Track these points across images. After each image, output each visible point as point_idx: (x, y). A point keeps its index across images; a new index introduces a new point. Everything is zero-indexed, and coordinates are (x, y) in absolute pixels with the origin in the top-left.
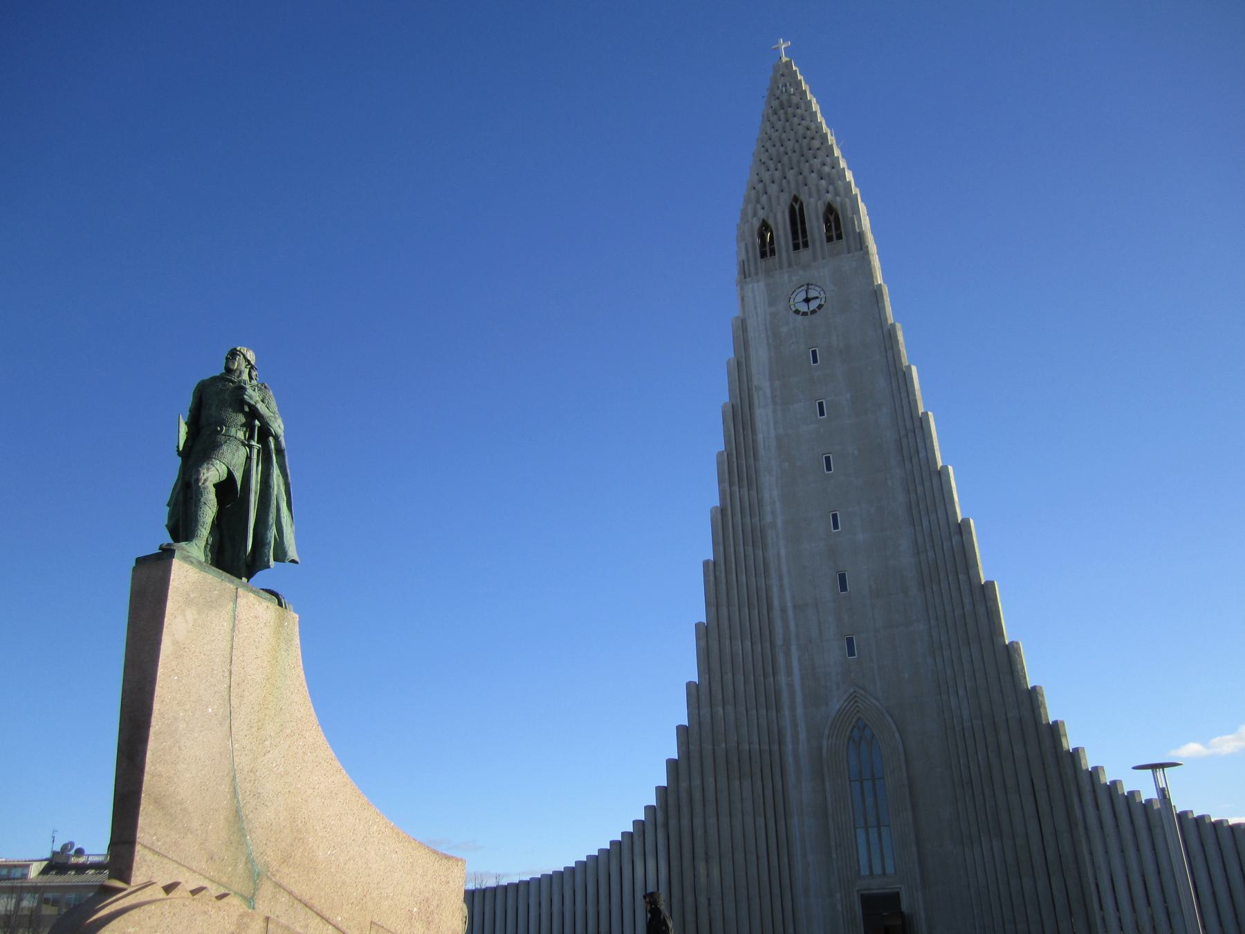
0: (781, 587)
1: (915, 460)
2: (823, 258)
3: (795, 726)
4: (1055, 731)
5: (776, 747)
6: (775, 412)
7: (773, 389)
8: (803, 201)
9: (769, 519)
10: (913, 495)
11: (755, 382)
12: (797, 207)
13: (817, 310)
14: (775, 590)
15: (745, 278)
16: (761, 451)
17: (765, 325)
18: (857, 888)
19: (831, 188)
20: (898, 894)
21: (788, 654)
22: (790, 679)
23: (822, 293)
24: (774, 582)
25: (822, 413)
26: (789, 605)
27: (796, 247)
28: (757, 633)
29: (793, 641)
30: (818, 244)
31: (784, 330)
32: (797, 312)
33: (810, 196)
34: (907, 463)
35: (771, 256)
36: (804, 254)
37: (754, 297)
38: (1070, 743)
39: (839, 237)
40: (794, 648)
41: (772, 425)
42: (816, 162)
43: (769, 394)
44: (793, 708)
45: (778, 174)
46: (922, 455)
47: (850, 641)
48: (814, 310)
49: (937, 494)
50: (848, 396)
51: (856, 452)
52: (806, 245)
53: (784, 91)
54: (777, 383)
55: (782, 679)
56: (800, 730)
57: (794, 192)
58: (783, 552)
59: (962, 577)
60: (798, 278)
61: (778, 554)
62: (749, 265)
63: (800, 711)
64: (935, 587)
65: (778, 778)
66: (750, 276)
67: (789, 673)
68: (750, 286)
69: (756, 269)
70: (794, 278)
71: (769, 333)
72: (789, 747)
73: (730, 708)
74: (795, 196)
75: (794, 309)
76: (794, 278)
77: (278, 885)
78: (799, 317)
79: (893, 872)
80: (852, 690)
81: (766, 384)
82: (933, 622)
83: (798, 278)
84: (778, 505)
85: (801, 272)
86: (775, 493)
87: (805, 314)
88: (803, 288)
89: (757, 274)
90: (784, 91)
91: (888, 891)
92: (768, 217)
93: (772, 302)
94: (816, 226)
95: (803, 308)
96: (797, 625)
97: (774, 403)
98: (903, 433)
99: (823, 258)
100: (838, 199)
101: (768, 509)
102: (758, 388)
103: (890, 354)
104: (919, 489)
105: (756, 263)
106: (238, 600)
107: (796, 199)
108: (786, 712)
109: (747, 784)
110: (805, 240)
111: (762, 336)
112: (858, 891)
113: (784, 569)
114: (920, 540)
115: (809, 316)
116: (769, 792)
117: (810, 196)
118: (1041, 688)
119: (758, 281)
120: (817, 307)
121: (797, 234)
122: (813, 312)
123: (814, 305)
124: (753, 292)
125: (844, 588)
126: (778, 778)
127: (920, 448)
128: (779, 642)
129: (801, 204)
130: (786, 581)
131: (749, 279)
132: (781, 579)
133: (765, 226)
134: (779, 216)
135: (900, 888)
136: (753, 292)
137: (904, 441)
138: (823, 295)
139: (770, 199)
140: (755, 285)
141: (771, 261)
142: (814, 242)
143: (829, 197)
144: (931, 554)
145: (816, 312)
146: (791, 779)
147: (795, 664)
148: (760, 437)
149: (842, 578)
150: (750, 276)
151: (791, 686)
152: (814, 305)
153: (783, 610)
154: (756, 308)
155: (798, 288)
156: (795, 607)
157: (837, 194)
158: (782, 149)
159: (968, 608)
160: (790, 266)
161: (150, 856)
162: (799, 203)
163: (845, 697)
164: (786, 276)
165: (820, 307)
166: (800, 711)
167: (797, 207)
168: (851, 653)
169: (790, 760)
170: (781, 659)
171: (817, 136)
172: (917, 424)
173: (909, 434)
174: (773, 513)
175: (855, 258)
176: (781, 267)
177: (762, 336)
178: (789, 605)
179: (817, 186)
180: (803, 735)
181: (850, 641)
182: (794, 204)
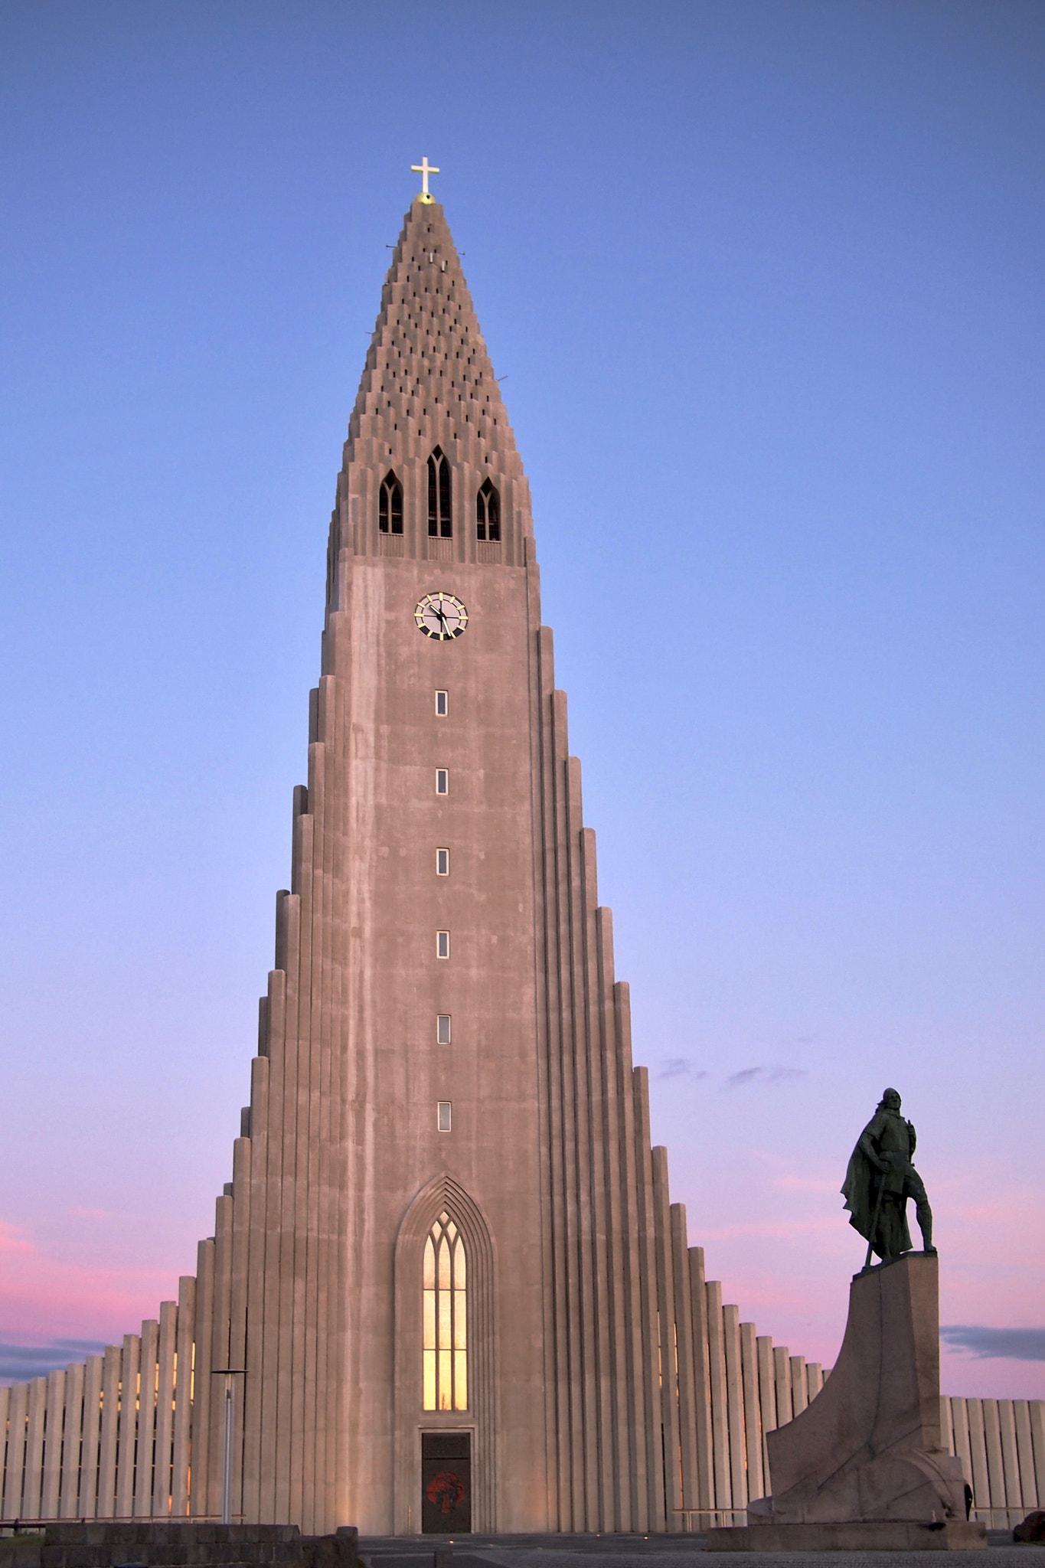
0: (361, 1021)
2: (473, 561)
3: (360, 1211)
5: (335, 1237)
6: (377, 769)
7: (378, 735)
8: (450, 460)
9: (354, 922)
10: (551, 933)
11: (354, 720)
12: (437, 464)
14: (352, 1024)
15: (356, 554)
16: (353, 824)
17: (378, 636)
18: (419, 1426)
19: (494, 455)
24: (352, 1013)
25: (442, 789)
26: (369, 1047)
27: (432, 531)
28: (326, 1081)
29: (370, 1097)
30: (467, 533)
31: (404, 652)
32: (425, 630)
33: (465, 459)
34: (550, 889)
35: (394, 531)
37: (366, 587)
38: (709, 1274)
39: (495, 534)
40: (369, 1107)
41: (371, 786)
42: (477, 404)
43: (371, 740)
44: (360, 1187)
45: (418, 402)
46: (576, 883)
50: (481, 773)
51: (482, 857)
52: (447, 532)
53: (431, 261)
54: (385, 729)
55: (350, 1145)
58: (368, 973)
59: (610, 1056)
60: (432, 578)
61: (362, 973)
62: (364, 536)
63: (369, 1192)
64: (567, 1059)
65: (334, 1277)
66: (364, 553)
67: (360, 1141)
68: (362, 568)
69: (375, 544)
70: (427, 578)
71: (382, 649)
72: (350, 1239)
73: (289, 1179)
74: (438, 447)
76: (427, 578)
79: (465, 1409)
80: (443, 1175)
81: (369, 726)
82: (555, 1103)
83: (432, 578)
84: (368, 904)
85: (437, 572)
86: (366, 887)
87: (435, 636)
88: (435, 597)
90: (431, 261)
92: (400, 468)
93: (390, 606)
94: (464, 508)
95: (434, 626)
96: (376, 1077)
97: (378, 757)
98: (549, 845)
100: (503, 477)
101: (353, 908)
102: (359, 729)
104: (563, 928)
105: (375, 535)
107: (437, 451)
108: (351, 1192)
109: (300, 1285)
110: (445, 519)
111: (371, 651)
114: (553, 992)
118: (684, 1206)
119: (374, 565)
121: (435, 510)
124: (365, 580)
128: (351, 1096)
129: (445, 466)
130: (368, 1014)
131: (359, 557)
132: (361, 1010)
133: (391, 478)
134: (417, 471)
135: (473, 1428)
136: (365, 580)
139: (405, 442)
140: (369, 570)
141: (390, 537)
142: (461, 529)
143: (491, 470)
146: (349, 1281)
148: (353, 801)
150: (364, 553)
151: (360, 1158)
152: (450, 627)
153: (361, 1053)
154: (366, 605)
155: (430, 595)
156: (376, 1052)
158: (426, 362)
159: (611, 1094)
160: (424, 557)
163: (434, 1181)
164: (415, 572)
165: (458, 632)
166: (369, 1192)
167: (437, 464)
169: (350, 1254)
170: (351, 1119)
172: (574, 841)
174: (360, 916)
175: (514, 576)
177: (371, 651)
178: (369, 1047)
180: (369, 1225)
182: (434, 457)
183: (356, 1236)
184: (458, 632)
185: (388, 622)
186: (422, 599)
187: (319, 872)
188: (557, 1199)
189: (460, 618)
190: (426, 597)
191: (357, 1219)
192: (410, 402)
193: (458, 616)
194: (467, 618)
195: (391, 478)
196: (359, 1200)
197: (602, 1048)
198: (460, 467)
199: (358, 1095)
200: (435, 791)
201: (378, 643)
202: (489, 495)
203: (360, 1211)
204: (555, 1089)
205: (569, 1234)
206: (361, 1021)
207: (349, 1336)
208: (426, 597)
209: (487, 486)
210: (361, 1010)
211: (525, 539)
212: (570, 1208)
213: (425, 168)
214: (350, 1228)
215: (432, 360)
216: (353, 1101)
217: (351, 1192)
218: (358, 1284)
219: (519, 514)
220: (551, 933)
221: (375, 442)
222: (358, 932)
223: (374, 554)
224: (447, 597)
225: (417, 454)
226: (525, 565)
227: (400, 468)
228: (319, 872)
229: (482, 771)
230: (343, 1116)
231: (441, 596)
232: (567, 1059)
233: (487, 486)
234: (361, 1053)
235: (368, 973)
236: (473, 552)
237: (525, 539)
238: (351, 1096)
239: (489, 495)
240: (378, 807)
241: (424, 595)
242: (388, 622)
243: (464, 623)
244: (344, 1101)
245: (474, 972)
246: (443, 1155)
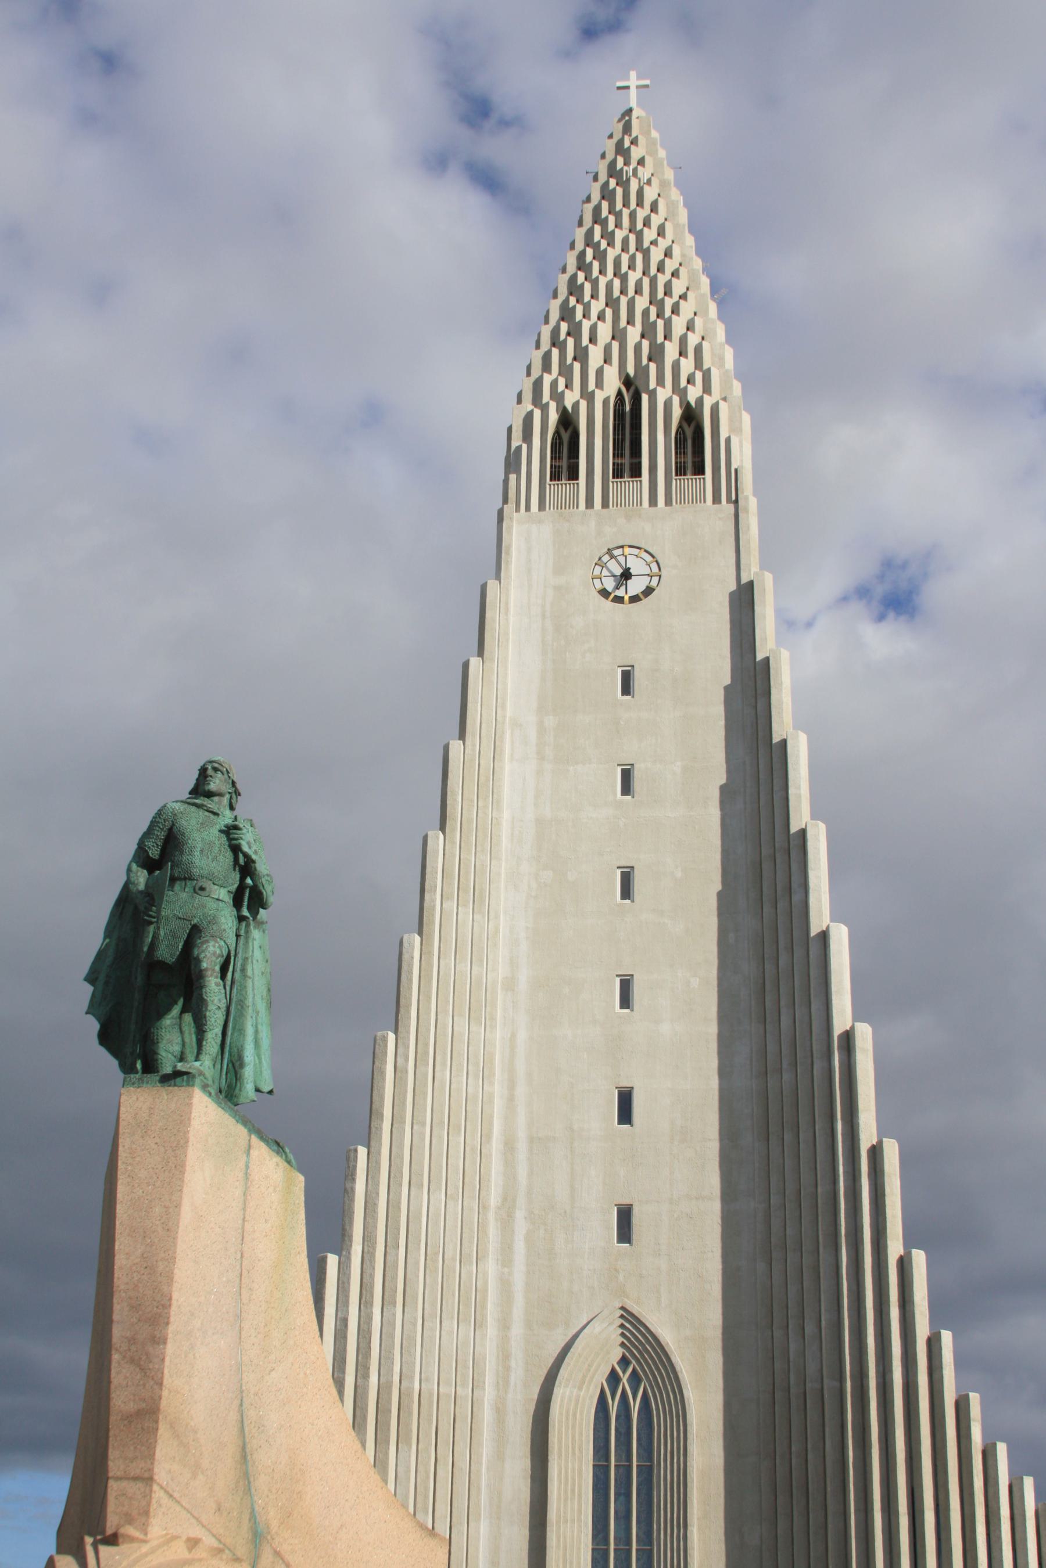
1: (782, 905)
5: (465, 1392)
7: (541, 730)
10: (769, 967)
11: (509, 713)
13: (641, 596)
22: (506, 1270)
23: (654, 566)
24: (498, 1089)
26: (522, 1134)
29: (521, 1201)
40: (520, 1215)
44: (505, 1324)
46: (796, 898)
48: (637, 595)
51: (679, 874)
54: (550, 721)
55: (491, 1267)
56: (513, 1364)
61: (513, 1036)
63: (517, 1330)
64: (788, 1137)
65: (463, 1448)
66: (528, 508)
72: (488, 1394)
75: (599, 586)
77: (277, 1554)
78: (608, 604)
82: (775, 1200)
93: (559, 569)
97: (541, 757)
99: (668, 502)
100: (708, 402)
106: (252, 1151)
108: (491, 1330)
110: (635, 461)
113: (521, 1067)
114: (771, 1048)
115: (627, 607)
116: (444, 1473)
117: (661, 382)
122: (634, 599)
123: (636, 586)
126: (463, 1448)
127: (794, 885)
128: (494, 1199)
133: (567, 421)
137: (767, 867)
141: (565, 486)
143: (693, 394)
144: (786, 1076)
146: (486, 1450)
148: (506, 815)
152: (636, 586)
156: (531, 1140)
157: (707, 389)
160: (605, 504)
161: (165, 1500)
164: (593, 524)
165: (648, 591)
169: (487, 1415)
171: (683, 271)
173: (777, 855)
176: (590, 503)
178: (522, 1134)
179: (676, 367)
180: (517, 1375)
183: (498, 1391)
185: (557, 588)
187: (451, 905)
188: (778, 1334)
191: (500, 1368)
192: (593, 329)
193: (648, 572)
195: (567, 421)
196: (504, 1342)
198: (653, 395)
199: (505, 1199)
200: (615, 795)
201: (544, 616)
202: (693, 425)
203: (505, 1356)
204: (774, 1179)
205: (792, 1382)
206: (511, 1099)
207: (483, 1528)
209: (691, 416)
210: (512, 1085)
211: (736, 470)
212: (793, 1347)
213: (633, 81)
214: (489, 1379)
215: (624, 279)
216: (499, 1208)
217: (491, 1330)
218: (499, 1456)
219: (728, 441)
220: (769, 967)
221: (547, 379)
222: (510, 985)
223: (542, 506)
225: (599, 384)
226: (736, 501)
227: (576, 405)
228: (451, 905)
229: (679, 763)
230: (482, 1226)
232: (788, 1137)
233: (691, 416)
234: (509, 1146)
235: (522, 1035)
237: (736, 470)
238: (494, 1199)
239: (693, 425)
240: (539, 822)
242: (557, 588)
244: (482, 1207)
245: (665, 1028)
246: (621, 1277)
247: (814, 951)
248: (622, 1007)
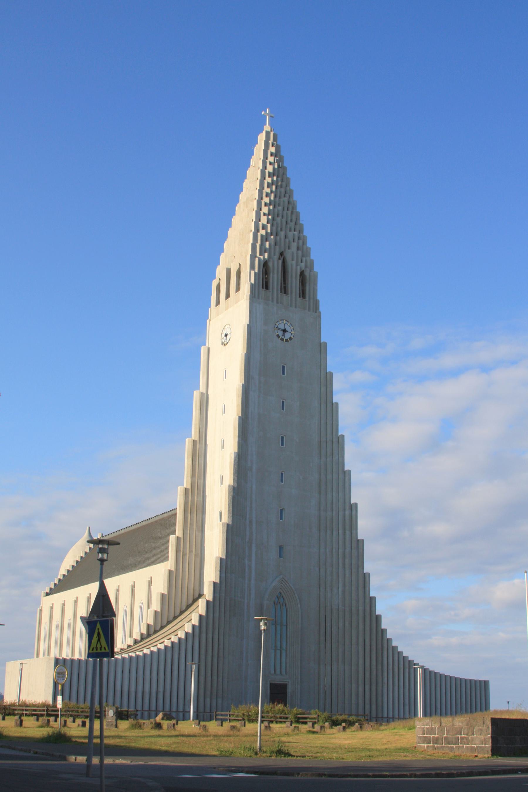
4: (378, 618)
18: (270, 680)
20: (287, 684)
21: (250, 548)
33: (293, 260)
36: (286, 299)
40: (254, 545)
44: (250, 580)
47: (281, 548)
49: (341, 484)
57: (282, 249)
58: (254, 487)
59: (348, 532)
63: (253, 582)
64: (329, 532)
67: (250, 560)
78: (279, 340)
88: (282, 321)
89: (258, 298)
91: (283, 683)
94: (294, 283)
103: (323, 389)
108: (247, 582)
112: (270, 681)
120: (289, 338)
122: (287, 340)
123: (287, 336)
125: (281, 518)
135: (289, 682)
138: (293, 332)
145: (288, 341)
147: (254, 555)
149: (281, 511)
151: (250, 567)
153: (251, 522)
155: (281, 320)
160: (277, 302)
162: (283, 257)
165: (291, 339)
166: (253, 582)
168: (280, 556)
180: (253, 596)
181: (281, 548)
184: (291, 339)
186: (278, 322)
189: (292, 332)
190: (279, 321)
194: (294, 333)
197: (344, 529)
208: (279, 321)
209: (302, 274)
224: (287, 323)
231: (285, 322)
233: (302, 274)
236: (296, 304)
238: (247, 540)
241: (278, 320)
243: (293, 335)
247: (341, 476)
248: (281, 482)
